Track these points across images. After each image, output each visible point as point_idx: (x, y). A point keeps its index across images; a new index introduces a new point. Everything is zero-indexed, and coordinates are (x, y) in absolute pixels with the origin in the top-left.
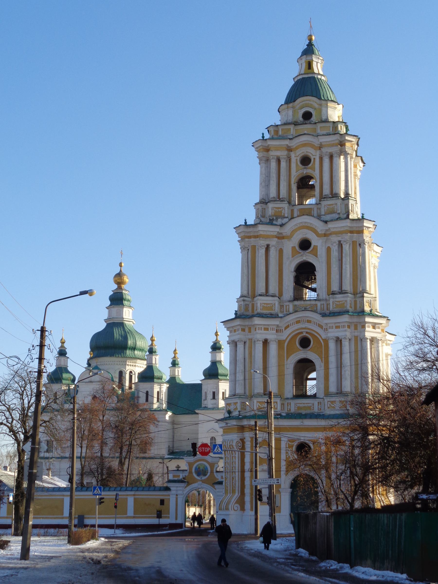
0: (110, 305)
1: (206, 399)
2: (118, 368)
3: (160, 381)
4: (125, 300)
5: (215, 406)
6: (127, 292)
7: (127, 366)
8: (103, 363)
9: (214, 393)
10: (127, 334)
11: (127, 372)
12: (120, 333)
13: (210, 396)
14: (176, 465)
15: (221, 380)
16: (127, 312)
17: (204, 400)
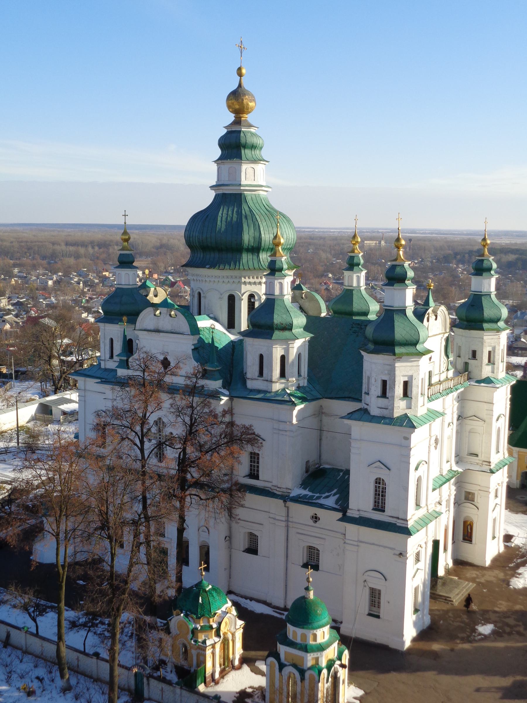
0: (220, 158)
1: (368, 394)
2: (226, 289)
3: (287, 333)
4: (245, 147)
5: (385, 413)
6: (252, 130)
7: (243, 286)
8: (201, 279)
9: (384, 383)
10: (244, 220)
11: (243, 298)
12: (229, 219)
13: (376, 389)
14: (312, 514)
15: (400, 357)
16: (250, 171)
17: (365, 393)
